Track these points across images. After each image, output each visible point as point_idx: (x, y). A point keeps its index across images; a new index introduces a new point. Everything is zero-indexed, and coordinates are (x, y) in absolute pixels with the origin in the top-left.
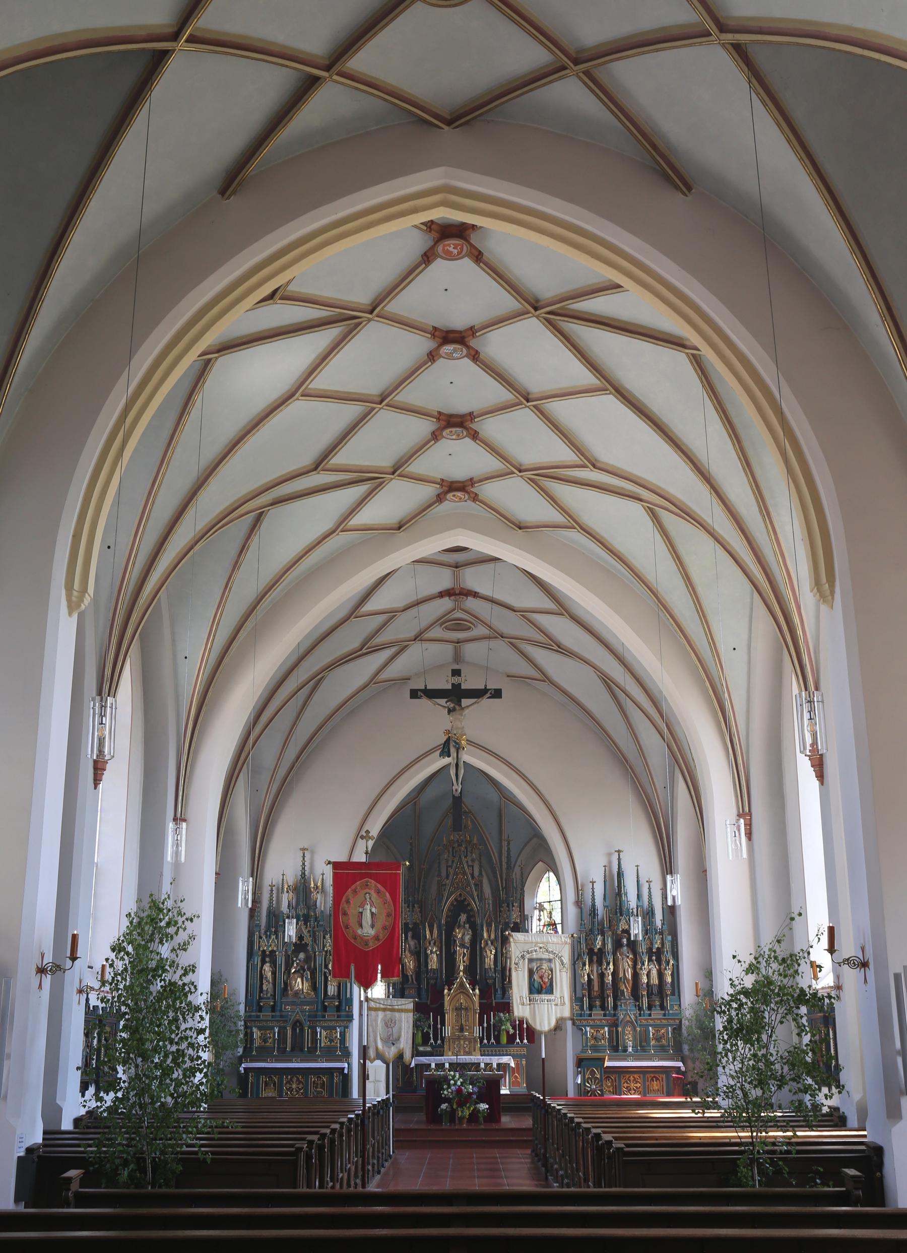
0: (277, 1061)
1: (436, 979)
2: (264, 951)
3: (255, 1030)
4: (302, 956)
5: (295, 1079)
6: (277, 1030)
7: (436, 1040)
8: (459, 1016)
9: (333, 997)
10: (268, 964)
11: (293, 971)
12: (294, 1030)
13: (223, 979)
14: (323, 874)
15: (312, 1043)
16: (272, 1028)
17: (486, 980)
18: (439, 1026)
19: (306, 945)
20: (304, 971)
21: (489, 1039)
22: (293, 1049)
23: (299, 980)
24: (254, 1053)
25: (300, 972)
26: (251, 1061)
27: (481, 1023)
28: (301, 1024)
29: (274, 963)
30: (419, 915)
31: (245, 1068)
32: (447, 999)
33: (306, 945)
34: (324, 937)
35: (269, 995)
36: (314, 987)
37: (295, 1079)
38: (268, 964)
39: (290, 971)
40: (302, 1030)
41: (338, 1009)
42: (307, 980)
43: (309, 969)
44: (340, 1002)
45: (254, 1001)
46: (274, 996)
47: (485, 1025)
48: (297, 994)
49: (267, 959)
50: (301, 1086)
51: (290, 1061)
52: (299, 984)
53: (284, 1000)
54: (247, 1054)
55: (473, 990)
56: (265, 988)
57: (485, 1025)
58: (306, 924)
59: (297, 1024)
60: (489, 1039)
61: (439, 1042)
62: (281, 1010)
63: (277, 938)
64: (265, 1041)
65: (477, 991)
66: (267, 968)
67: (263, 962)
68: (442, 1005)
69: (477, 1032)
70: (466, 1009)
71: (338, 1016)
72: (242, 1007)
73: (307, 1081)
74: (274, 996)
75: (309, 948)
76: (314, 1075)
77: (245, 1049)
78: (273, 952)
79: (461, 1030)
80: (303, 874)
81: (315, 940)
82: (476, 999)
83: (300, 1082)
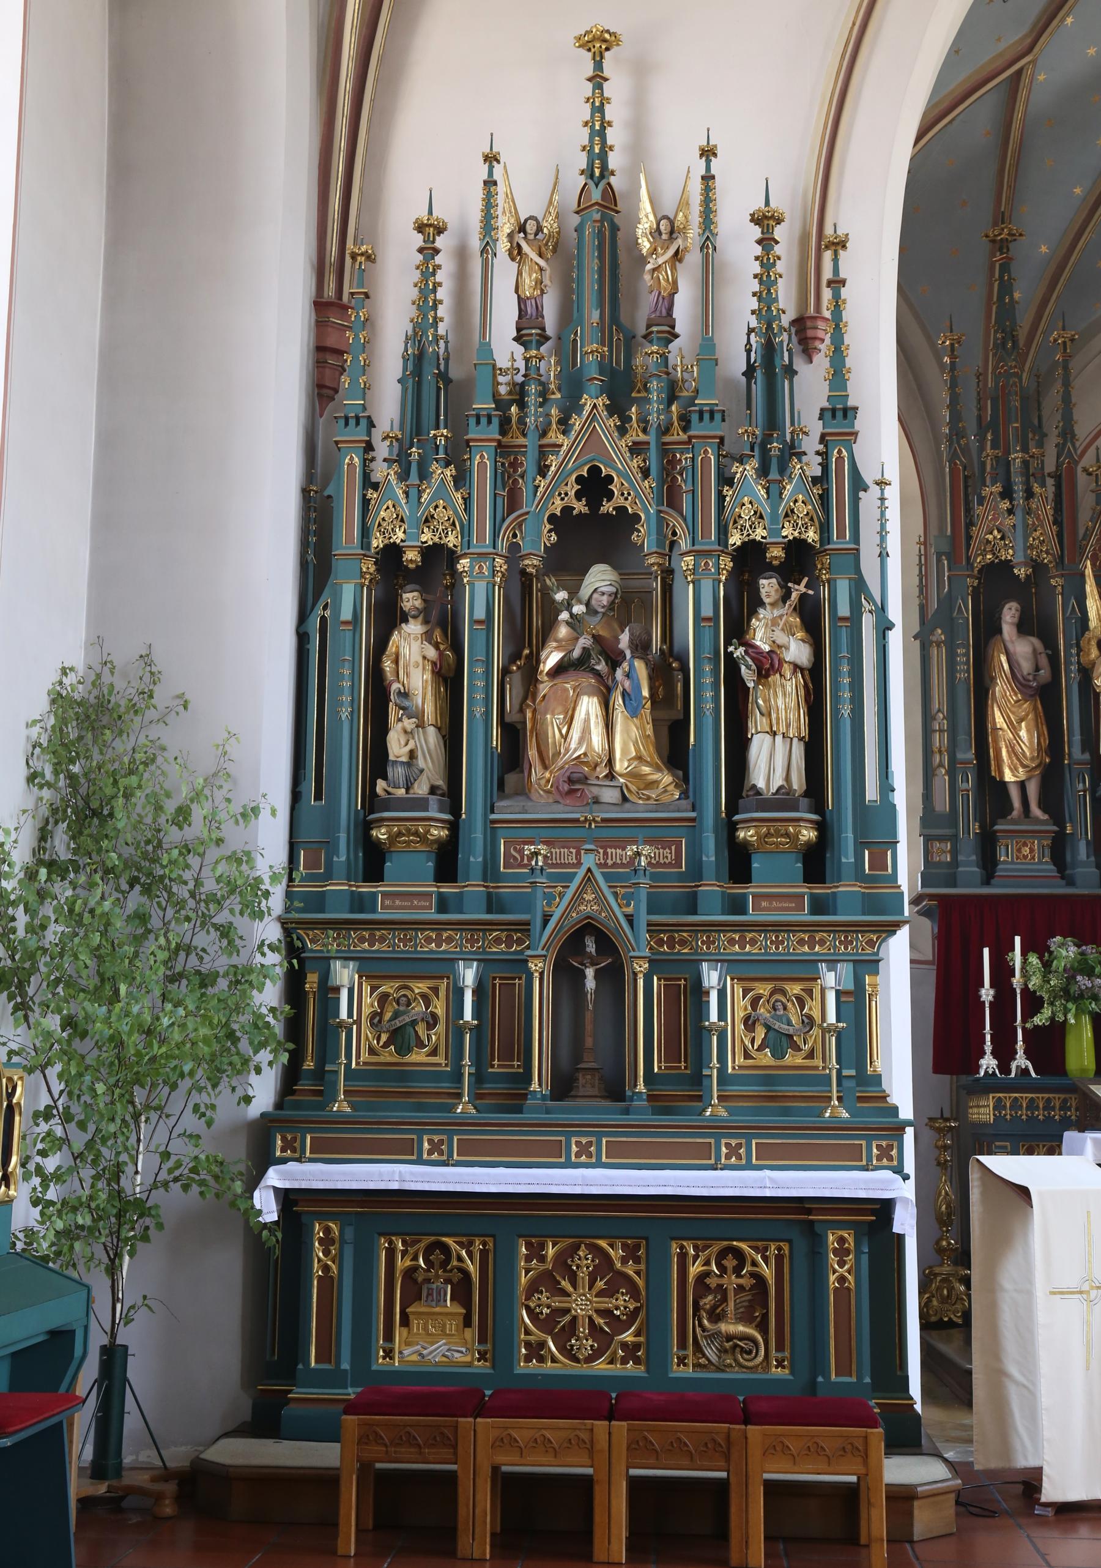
0: (476, 1153)
2: (393, 552)
3: (344, 974)
4: (600, 579)
5: (584, 1262)
6: (469, 976)
9: (783, 800)
10: (414, 628)
11: (552, 659)
12: (566, 974)
13: (162, 696)
14: (708, 153)
15: (672, 1053)
16: (441, 969)
19: (626, 520)
20: (614, 662)
22: (563, 1087)
23: (589, 707)
24: (341, 1106)
25: (595, 665)
26: (330, 1150)
28: (607, 944)
29: (446, 626)
30: (1051, 530)
31: (287, 1198)
33: (626, 520)
34: (725, 480)
35: (421, 789)
36: (674, 750)
37: (584, 1262)
38: (414, 628)
39: (534, 662)
40: (614, 976)
41: (816, 863)
42: (633, 712)
43: (641, 647)
44: (822, 827)
45: (347, 809)
46: (451, 793)
48: (575, 782)
49: (411, 600)
50: (622, 1303)
51: (552, 1154)
52: (592, 729)
53: (507, 810)
54: (300, 1115)
56: (397, 746)
58: (617, 409)
59: (588, 943)
62: (490, 872)
63: (460, 480)
64: (401, 1038)
66: (412, 650)
67: (388, 618)
71: (819, 906)
72: (270, 842)
73: (656, 1273)
74: (451, 793)
75: (645, 536)
76: (702, 1241)
77: (291, 1077)
78: (438, 558)
80: (597, 169)
81: (670, 497)
83: (618, 1282)
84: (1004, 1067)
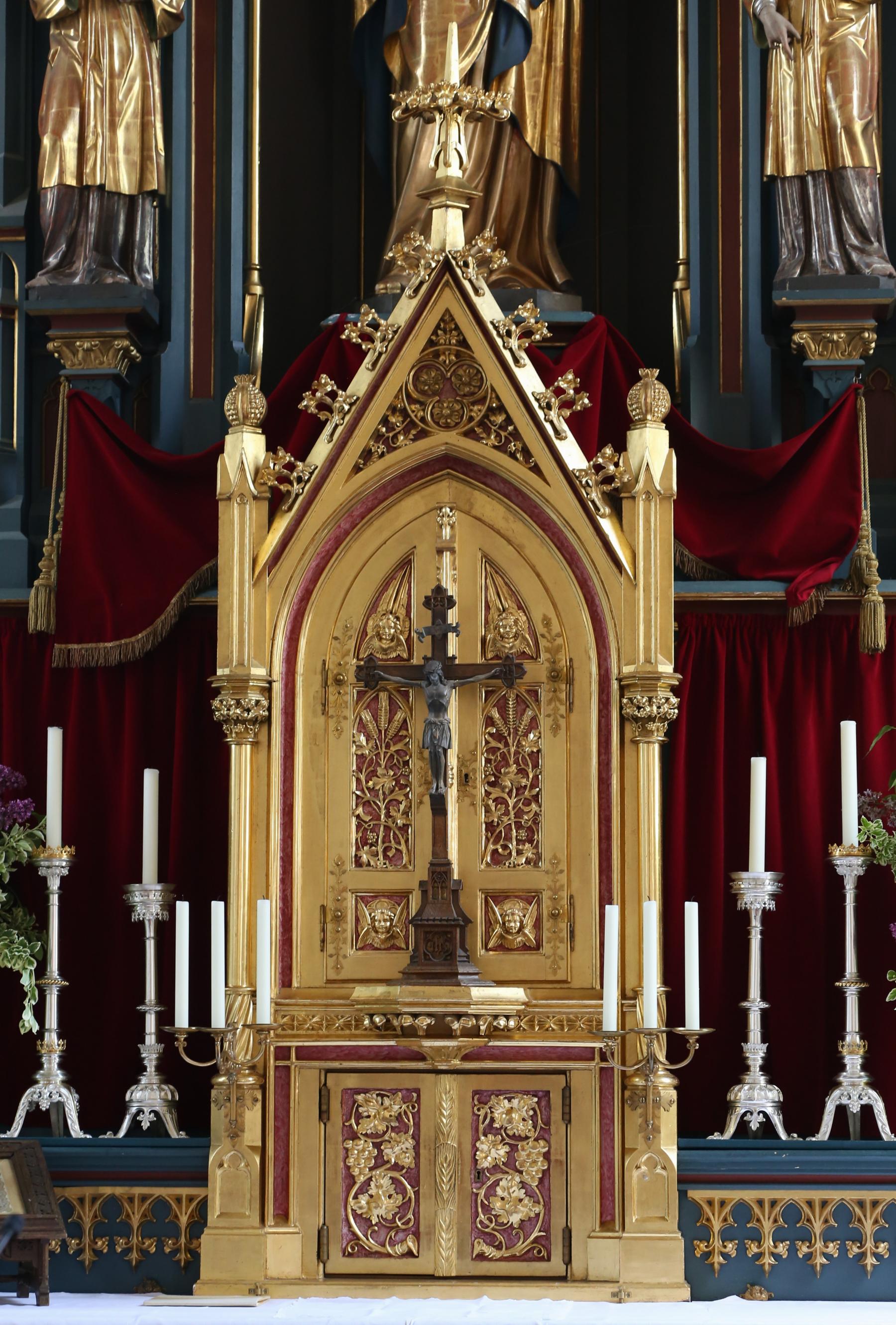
1: (150, 330)
7: (101, 1076)
8: (400, 771)
17: (779, 322)
18: (147, 899)
21: (804, 1076)
27: (699, 860)
32: (242, 535)
47: (758, 886)
55: (605, 428)
57: (758, 887)
60: (804, 1076)
61: (148, 1097)
65: (652, 448)
68: (200, 630)
69: (631, 964)
70: (502, 675)
79: (438, 941)
82: (646, 545)
84: (801, 1111)
